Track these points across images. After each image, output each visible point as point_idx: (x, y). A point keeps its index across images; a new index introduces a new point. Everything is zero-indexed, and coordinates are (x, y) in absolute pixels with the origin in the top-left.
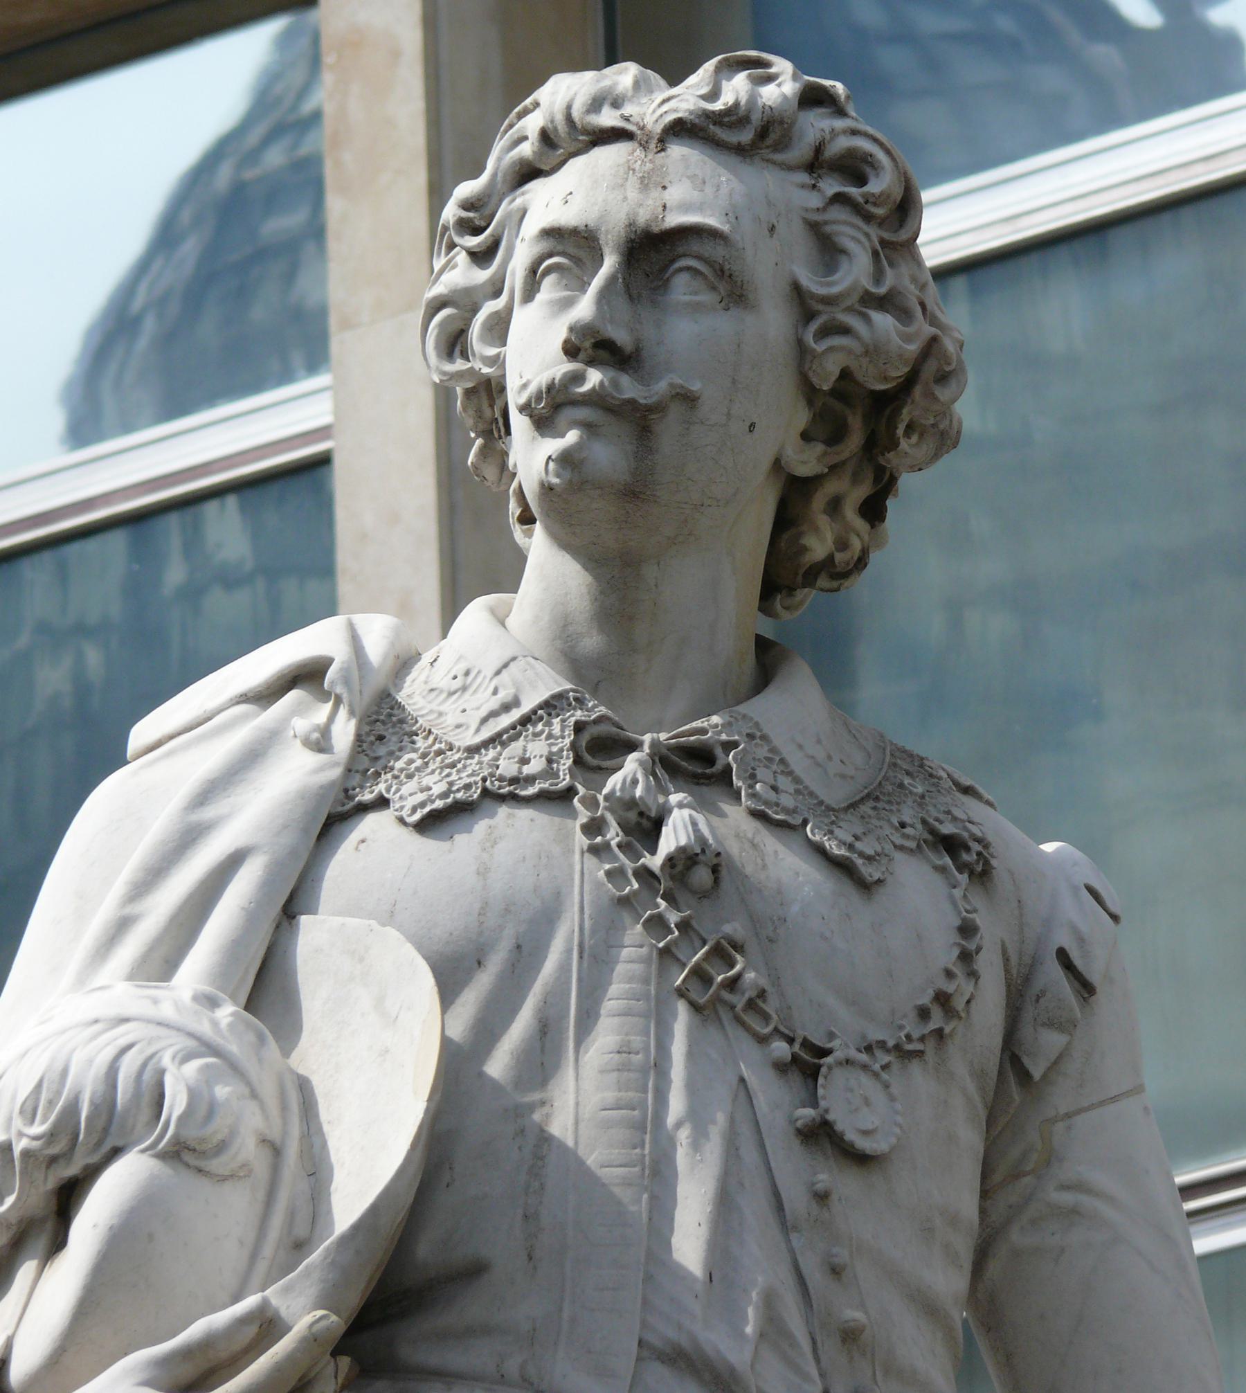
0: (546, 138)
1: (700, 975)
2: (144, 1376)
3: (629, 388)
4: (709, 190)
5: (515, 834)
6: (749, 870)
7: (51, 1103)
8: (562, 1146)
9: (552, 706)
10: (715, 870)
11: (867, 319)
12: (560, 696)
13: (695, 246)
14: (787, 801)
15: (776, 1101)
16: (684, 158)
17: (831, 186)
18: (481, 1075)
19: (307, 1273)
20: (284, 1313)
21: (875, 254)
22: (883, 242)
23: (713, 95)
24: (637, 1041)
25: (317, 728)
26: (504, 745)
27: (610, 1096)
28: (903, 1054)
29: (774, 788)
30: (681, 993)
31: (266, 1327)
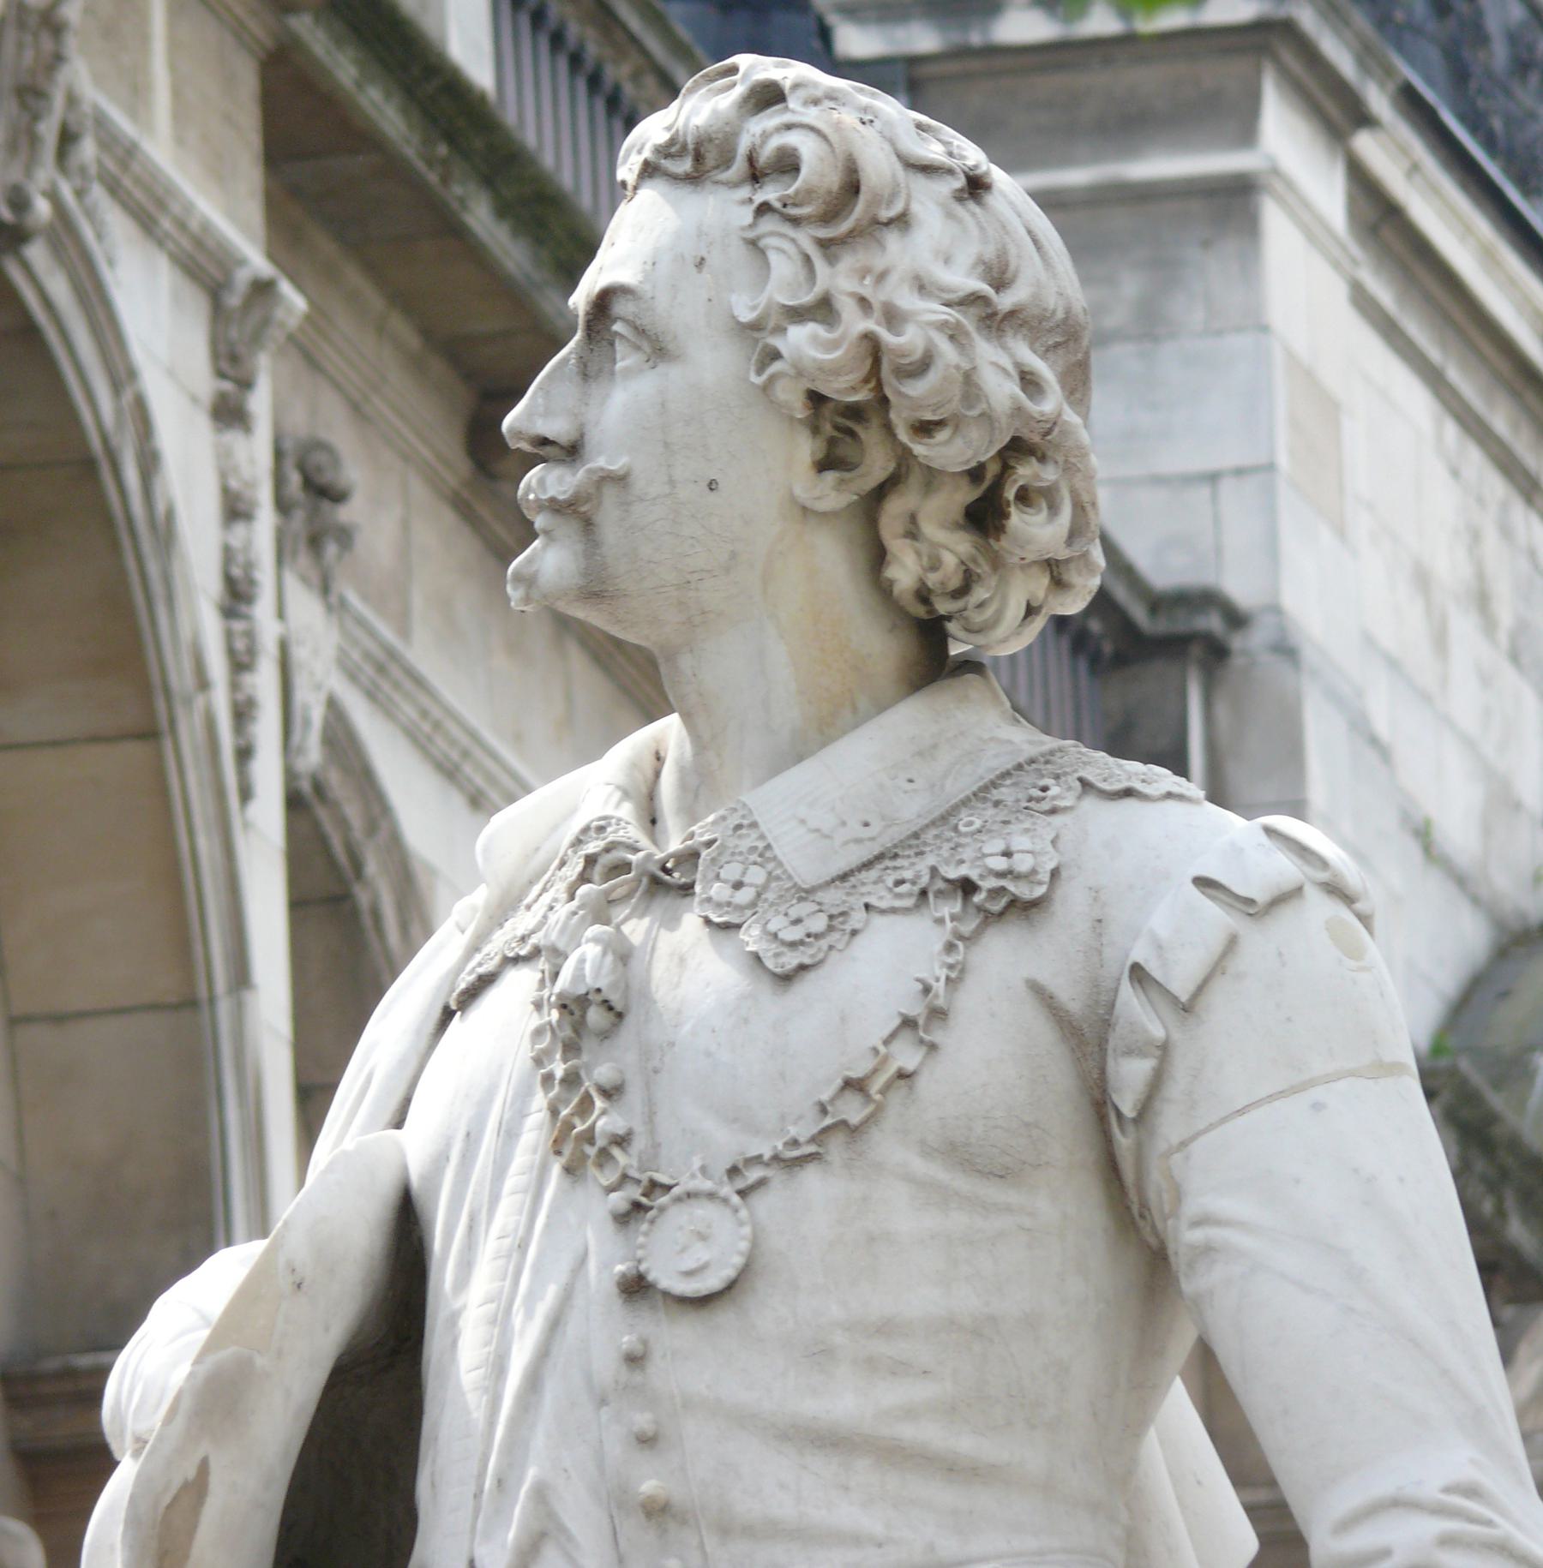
10: (607, 1005)
21: (807, 259)
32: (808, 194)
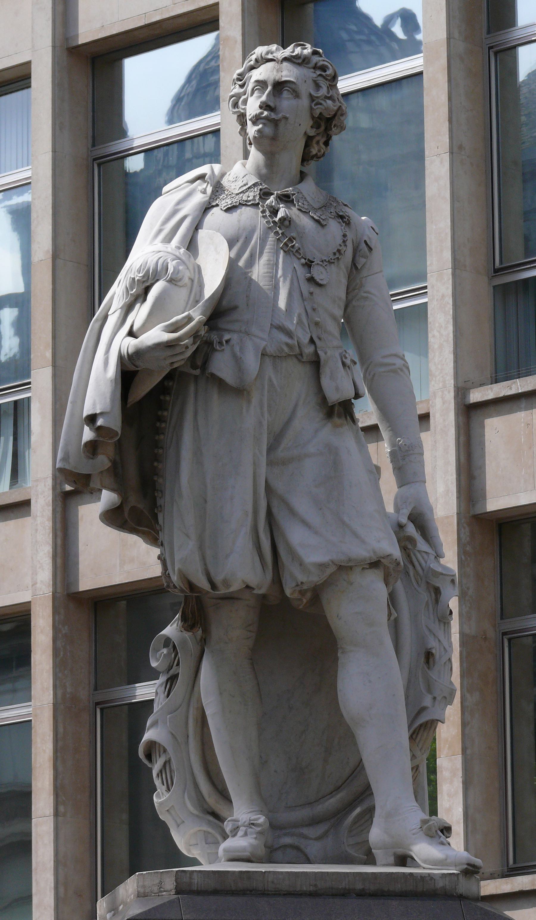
0: (256, 60)
1: (286, 244)
2: (162, 329)
3: (273, 116)
4: (292, 73)
5: (246, 213)
6: (297, 222)
7: (144, 269)
8: (255, 281)
9: (255, 185)
10: (290, 221)
11: (326, 101)
12: (257, 183)
13: (288, 85)
14: (306, 207)
15: (302, 272)
16: (286, 66)
17: (318, 72)
18: (238, 265)
19: (198, 307)
20: (193, 316)
21: (328, 87)
22: (329, 85)
23: (293, 52)
24: (272, 258)
25: (204, 189)
26: (244, 193)
27: (266, 270)
28: (330, 262)
29: (303, 204)
30: (282, 248)
31: (189, 319)
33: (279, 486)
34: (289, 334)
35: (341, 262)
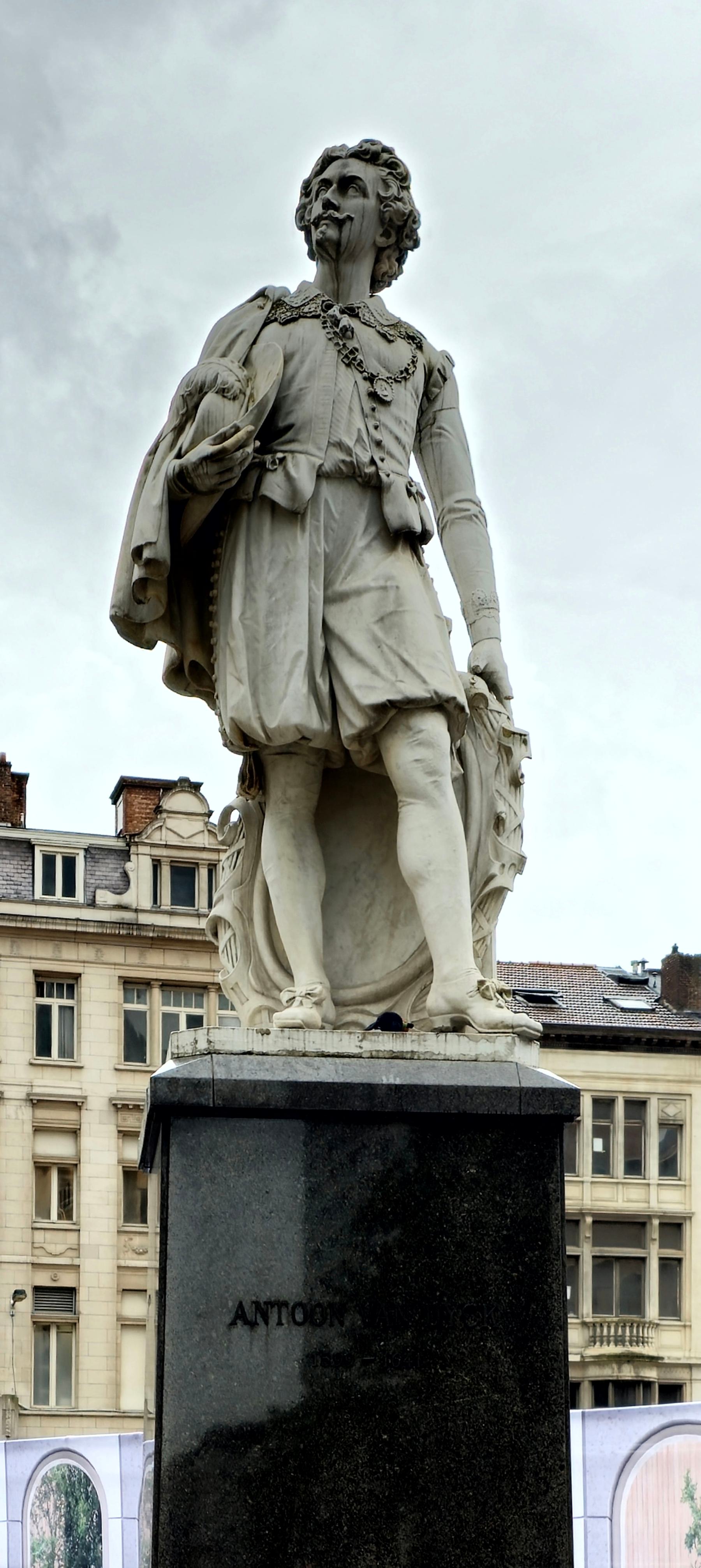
1: (346, 356)
10: (353, 332)
32: (398, 174)
33: (336, 624)
34: (349, 451)
35: (409, 384)
